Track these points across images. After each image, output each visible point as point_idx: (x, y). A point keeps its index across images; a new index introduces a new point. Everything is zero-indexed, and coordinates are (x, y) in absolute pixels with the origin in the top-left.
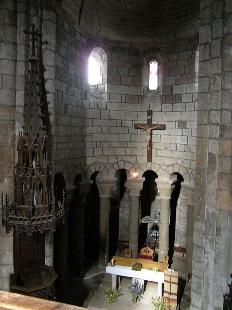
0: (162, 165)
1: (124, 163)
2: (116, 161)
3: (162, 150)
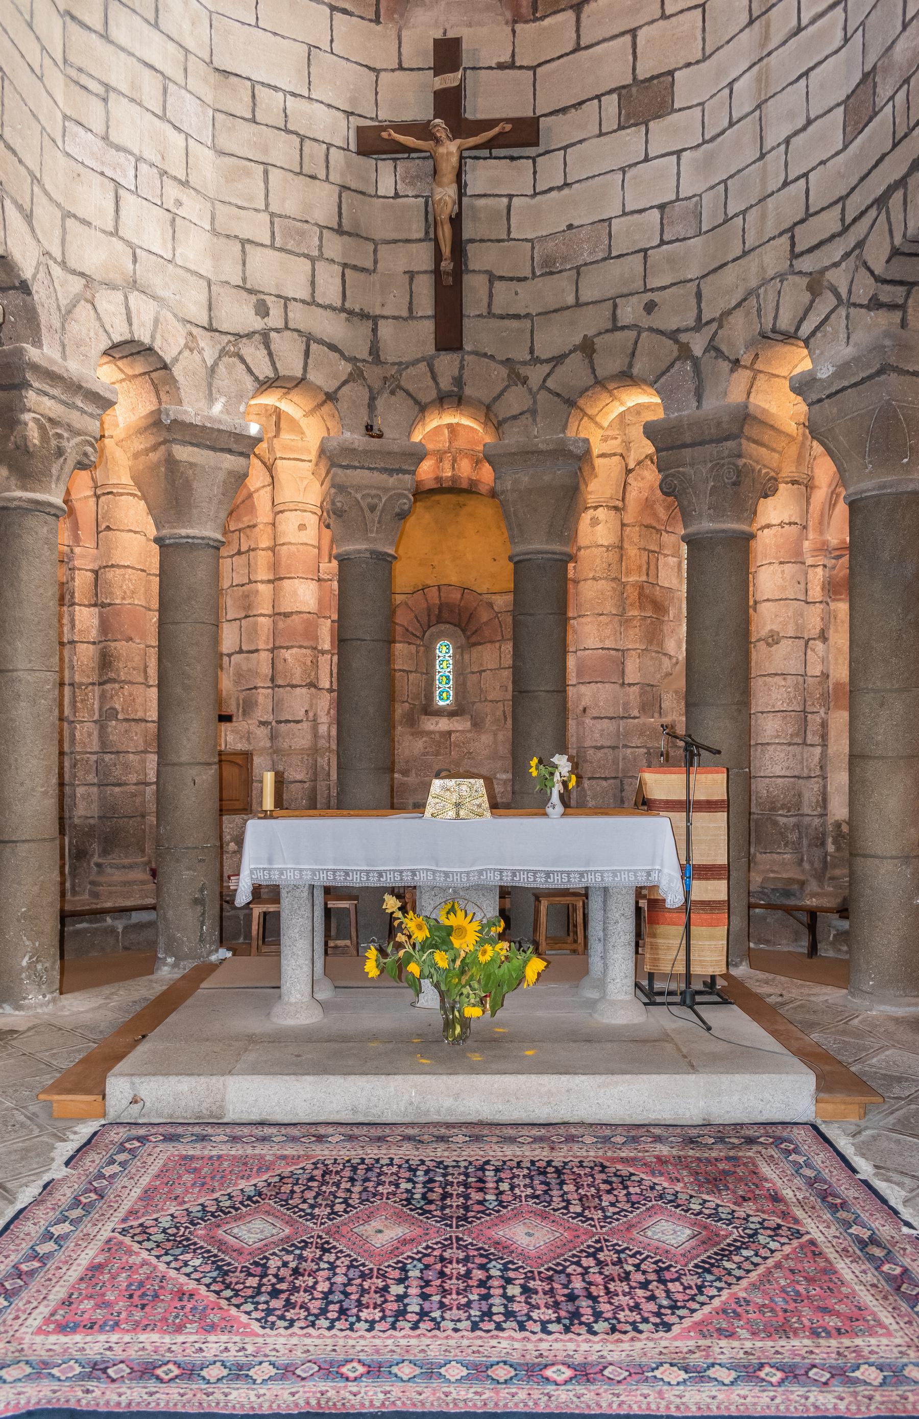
0: (524, 363)
1: (303, 347)
2: (258, 324)
3: (520, 280)
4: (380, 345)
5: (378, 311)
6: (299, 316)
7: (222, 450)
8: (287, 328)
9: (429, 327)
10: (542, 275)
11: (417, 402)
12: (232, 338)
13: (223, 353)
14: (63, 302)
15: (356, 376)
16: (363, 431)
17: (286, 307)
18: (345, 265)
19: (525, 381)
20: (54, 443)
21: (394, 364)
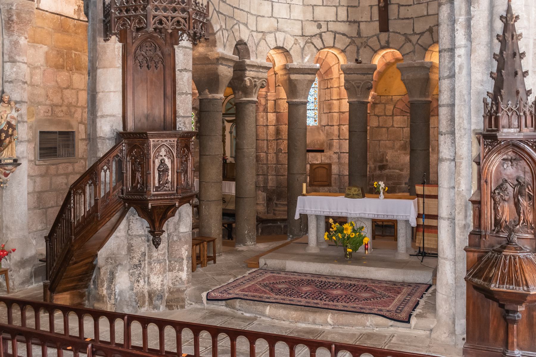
0: (411, 35)
1: (333, 36)
2: (318, 31)
3: (409, 6)
4: (361, 31)
5: (360, 20)
6: (332, 26)
7: (306, 74)
8: (328, 31)
9: (377, 24)
11: (373, 50)
13: (307, 42)
14: (256, 42)
15: (352, 43)
17: (327, 24)
18: (348, 6)
19: (410, 41)
20: (254, 83)
21: (365, 37)
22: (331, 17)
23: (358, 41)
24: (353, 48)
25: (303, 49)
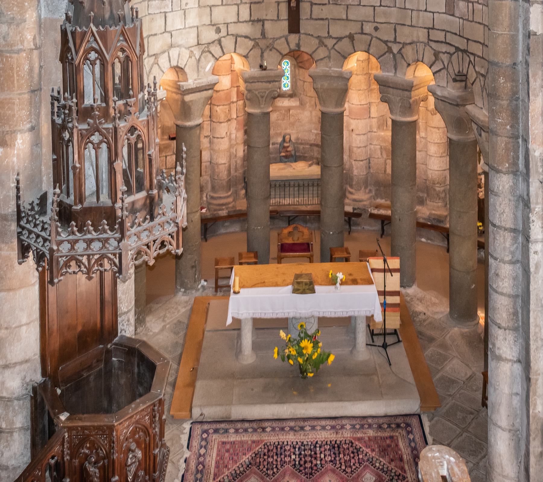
0: (325, 38)
1: (235, 40)
3: (323, 5)
4: (266, 31)
5: (264, 18)
6: (233, 29)
9: (285, 24)
10: (332, 4)
11: (281, 53)
12: (206, 45)
13: (203, 52)
16: (258, 67)
19: (326, 46)
21: (271, 39)
22: (232, 18)
23: (262, 43)
24: (257, 52)
25: (199, 60)
